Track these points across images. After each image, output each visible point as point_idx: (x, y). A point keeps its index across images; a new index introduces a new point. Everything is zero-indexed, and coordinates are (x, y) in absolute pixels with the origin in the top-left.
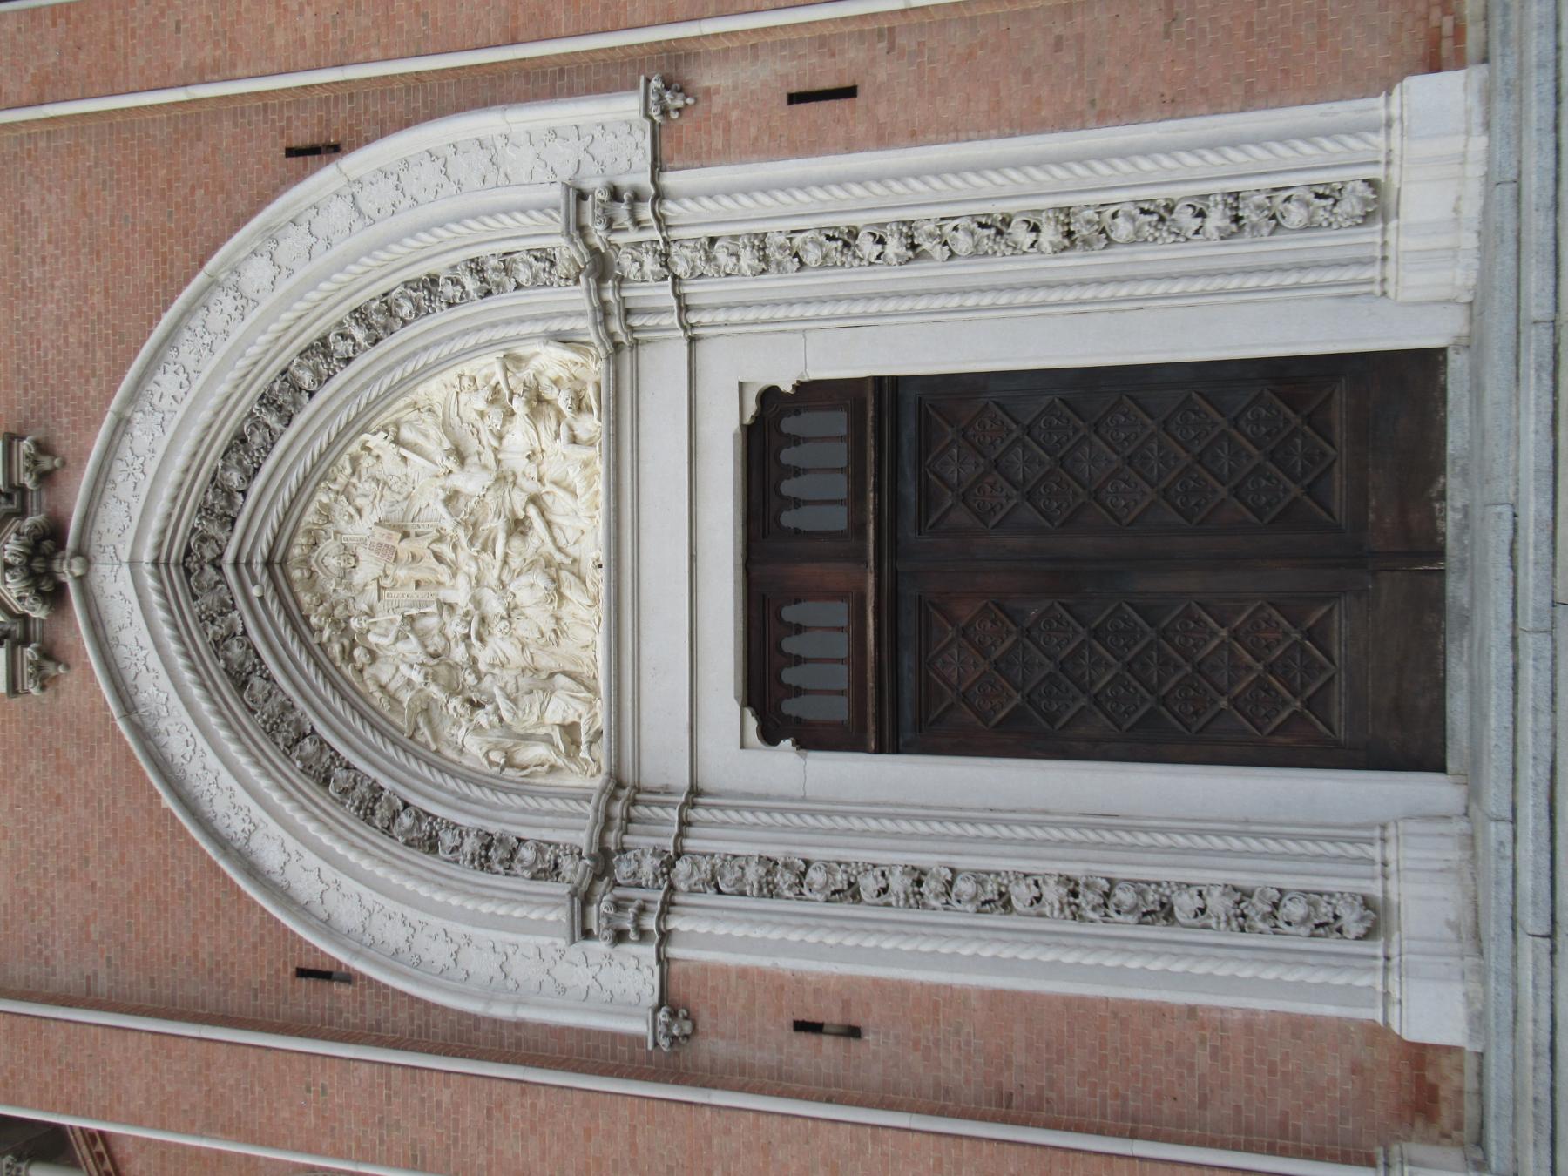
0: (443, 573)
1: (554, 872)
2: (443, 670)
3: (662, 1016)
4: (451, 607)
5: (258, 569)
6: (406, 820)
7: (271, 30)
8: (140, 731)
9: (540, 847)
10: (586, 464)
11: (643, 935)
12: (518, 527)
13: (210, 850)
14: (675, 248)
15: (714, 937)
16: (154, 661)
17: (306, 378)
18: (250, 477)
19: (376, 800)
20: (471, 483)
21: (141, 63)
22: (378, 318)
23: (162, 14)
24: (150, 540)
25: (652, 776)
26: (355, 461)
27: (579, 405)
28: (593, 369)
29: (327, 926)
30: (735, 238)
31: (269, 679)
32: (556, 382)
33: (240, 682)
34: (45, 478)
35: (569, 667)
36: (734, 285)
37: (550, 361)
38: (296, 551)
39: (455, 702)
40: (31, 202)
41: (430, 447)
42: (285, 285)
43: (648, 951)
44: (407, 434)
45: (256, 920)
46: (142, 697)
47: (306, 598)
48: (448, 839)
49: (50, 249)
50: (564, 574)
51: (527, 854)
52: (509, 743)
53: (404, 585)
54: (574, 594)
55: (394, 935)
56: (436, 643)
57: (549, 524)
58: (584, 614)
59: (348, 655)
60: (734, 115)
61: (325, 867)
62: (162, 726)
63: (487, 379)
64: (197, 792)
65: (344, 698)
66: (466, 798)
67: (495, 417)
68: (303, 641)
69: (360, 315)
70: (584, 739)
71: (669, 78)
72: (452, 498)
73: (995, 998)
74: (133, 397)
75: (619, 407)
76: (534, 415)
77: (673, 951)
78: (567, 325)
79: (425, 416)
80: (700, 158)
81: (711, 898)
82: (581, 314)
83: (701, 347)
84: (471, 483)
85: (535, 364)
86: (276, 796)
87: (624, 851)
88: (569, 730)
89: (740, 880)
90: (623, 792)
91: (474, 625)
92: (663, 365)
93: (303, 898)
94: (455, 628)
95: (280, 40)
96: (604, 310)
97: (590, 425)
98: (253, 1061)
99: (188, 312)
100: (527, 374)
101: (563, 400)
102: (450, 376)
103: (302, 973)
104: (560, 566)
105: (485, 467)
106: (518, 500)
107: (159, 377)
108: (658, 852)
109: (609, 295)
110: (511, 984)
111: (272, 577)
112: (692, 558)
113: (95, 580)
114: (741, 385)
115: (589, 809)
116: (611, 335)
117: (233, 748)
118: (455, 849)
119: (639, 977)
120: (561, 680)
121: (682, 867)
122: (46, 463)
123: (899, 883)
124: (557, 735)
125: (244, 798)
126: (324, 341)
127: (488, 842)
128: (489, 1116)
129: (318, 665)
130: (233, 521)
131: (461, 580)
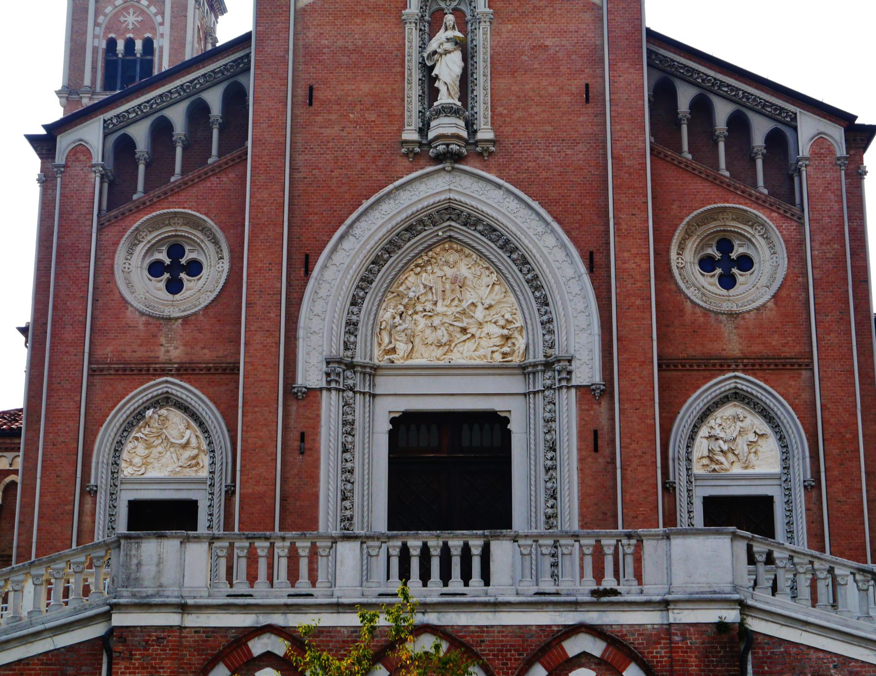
0: (448, 302)
1: (347, 348)
2: (413, 302)
3: (304, 390)
4: (435, 304)
5: (448, 234)
6: (361, 294)
7: (629, 251)
8: (390, 192)
9: (354, 343)
10: (485, 356)
11: (329, 382)
12: (464, 330)
13: (348, 222)
14: (552, 391)
15: (330, 407)
16: (415, 198)
17: (515, 256)
18: (480, 232)
19: (368, 282)
20: (480, 313)
21: (623, 199)
22: (535, 283)
23: (639, 208)
24: (457, 197)
25: (379, 380)
26: (488, 268)
27: (505, 355)
28: (516, 359)
29: (325, 266)
30: (555, 412)
31: (409, 240)
32: (514, 344)
35: (415, 349)
36: (541, 410)
37: (520, 343)
38: (455, 246)
39: (402, 308)
40: (580, 147)
41: (493, 296)
42: (545, 251)
43: (324, 385)
44: (497, 288)
45: (325, 238)
46: (402, 193)
47: (438, 249)
48: (355, 309)
49: (563, 154)
50: (447, 347)
51: (352, 339)
52: (388, 328)
53: (443, 287)
54: (440, 352)
55: (323, 293)
56: (423, 299)
57: (465, 341)
58: (434, 354)
59: (417, 266)
60: (592, 412)
61: (345, 266)
62: (392, 201)
63: (515, 319)
64: (369, 215)
65: (403, 267)
66: (369, 314)
67: (502, 322)
68: (422, 251)
69: (536, 277)
70: (391, 357)
71: (607, 391)
72: (473, 304)
73: (316, 496)
74: (508, 190)
75: (503, 369)
76: (502, 336)
77: (324, 393)
78: (531, 352)
79: (503, 295)
80: (579, 401)
81: (341, 404)
82: (534, 357)
83: (523, 397)
85: (520, 337)
86: (368, 247)
87: (355, 373)
88: (394, 350)
89: (348, 414)
90: (372, 371)
91: (430, 314)
92: (516, 384)
93: (334, 257)
94: (429, 306)
95: (626, 254)
96: (535, 365)
98: (277, 242)
99: (538, 214)
100: (516, 334)
101: (506, 349)
102: (516, 306)
103: (307, 256)
104: (450, 345)
105: (485, 317)
106: (472, 330)
107: (516, 201)
108: (355, 385)
109: (539, 368)
110: (309, 335)
111: (445, 238)
112: (453, 395)
113: (443, 173)
114: (510, 411)
115: (368, 360)
116: (527, 367)
117: (385, 230)
118: (353, 313)
119: (315, 381)
120: (410, 346)
121: (351, 394)
122: (486, 154)
124: (391, 346)
126: (528, 263)
127: (355, 324)
128: (267, 331)
129: (414, 257)
130: (465, 225)
131: (445, 309)
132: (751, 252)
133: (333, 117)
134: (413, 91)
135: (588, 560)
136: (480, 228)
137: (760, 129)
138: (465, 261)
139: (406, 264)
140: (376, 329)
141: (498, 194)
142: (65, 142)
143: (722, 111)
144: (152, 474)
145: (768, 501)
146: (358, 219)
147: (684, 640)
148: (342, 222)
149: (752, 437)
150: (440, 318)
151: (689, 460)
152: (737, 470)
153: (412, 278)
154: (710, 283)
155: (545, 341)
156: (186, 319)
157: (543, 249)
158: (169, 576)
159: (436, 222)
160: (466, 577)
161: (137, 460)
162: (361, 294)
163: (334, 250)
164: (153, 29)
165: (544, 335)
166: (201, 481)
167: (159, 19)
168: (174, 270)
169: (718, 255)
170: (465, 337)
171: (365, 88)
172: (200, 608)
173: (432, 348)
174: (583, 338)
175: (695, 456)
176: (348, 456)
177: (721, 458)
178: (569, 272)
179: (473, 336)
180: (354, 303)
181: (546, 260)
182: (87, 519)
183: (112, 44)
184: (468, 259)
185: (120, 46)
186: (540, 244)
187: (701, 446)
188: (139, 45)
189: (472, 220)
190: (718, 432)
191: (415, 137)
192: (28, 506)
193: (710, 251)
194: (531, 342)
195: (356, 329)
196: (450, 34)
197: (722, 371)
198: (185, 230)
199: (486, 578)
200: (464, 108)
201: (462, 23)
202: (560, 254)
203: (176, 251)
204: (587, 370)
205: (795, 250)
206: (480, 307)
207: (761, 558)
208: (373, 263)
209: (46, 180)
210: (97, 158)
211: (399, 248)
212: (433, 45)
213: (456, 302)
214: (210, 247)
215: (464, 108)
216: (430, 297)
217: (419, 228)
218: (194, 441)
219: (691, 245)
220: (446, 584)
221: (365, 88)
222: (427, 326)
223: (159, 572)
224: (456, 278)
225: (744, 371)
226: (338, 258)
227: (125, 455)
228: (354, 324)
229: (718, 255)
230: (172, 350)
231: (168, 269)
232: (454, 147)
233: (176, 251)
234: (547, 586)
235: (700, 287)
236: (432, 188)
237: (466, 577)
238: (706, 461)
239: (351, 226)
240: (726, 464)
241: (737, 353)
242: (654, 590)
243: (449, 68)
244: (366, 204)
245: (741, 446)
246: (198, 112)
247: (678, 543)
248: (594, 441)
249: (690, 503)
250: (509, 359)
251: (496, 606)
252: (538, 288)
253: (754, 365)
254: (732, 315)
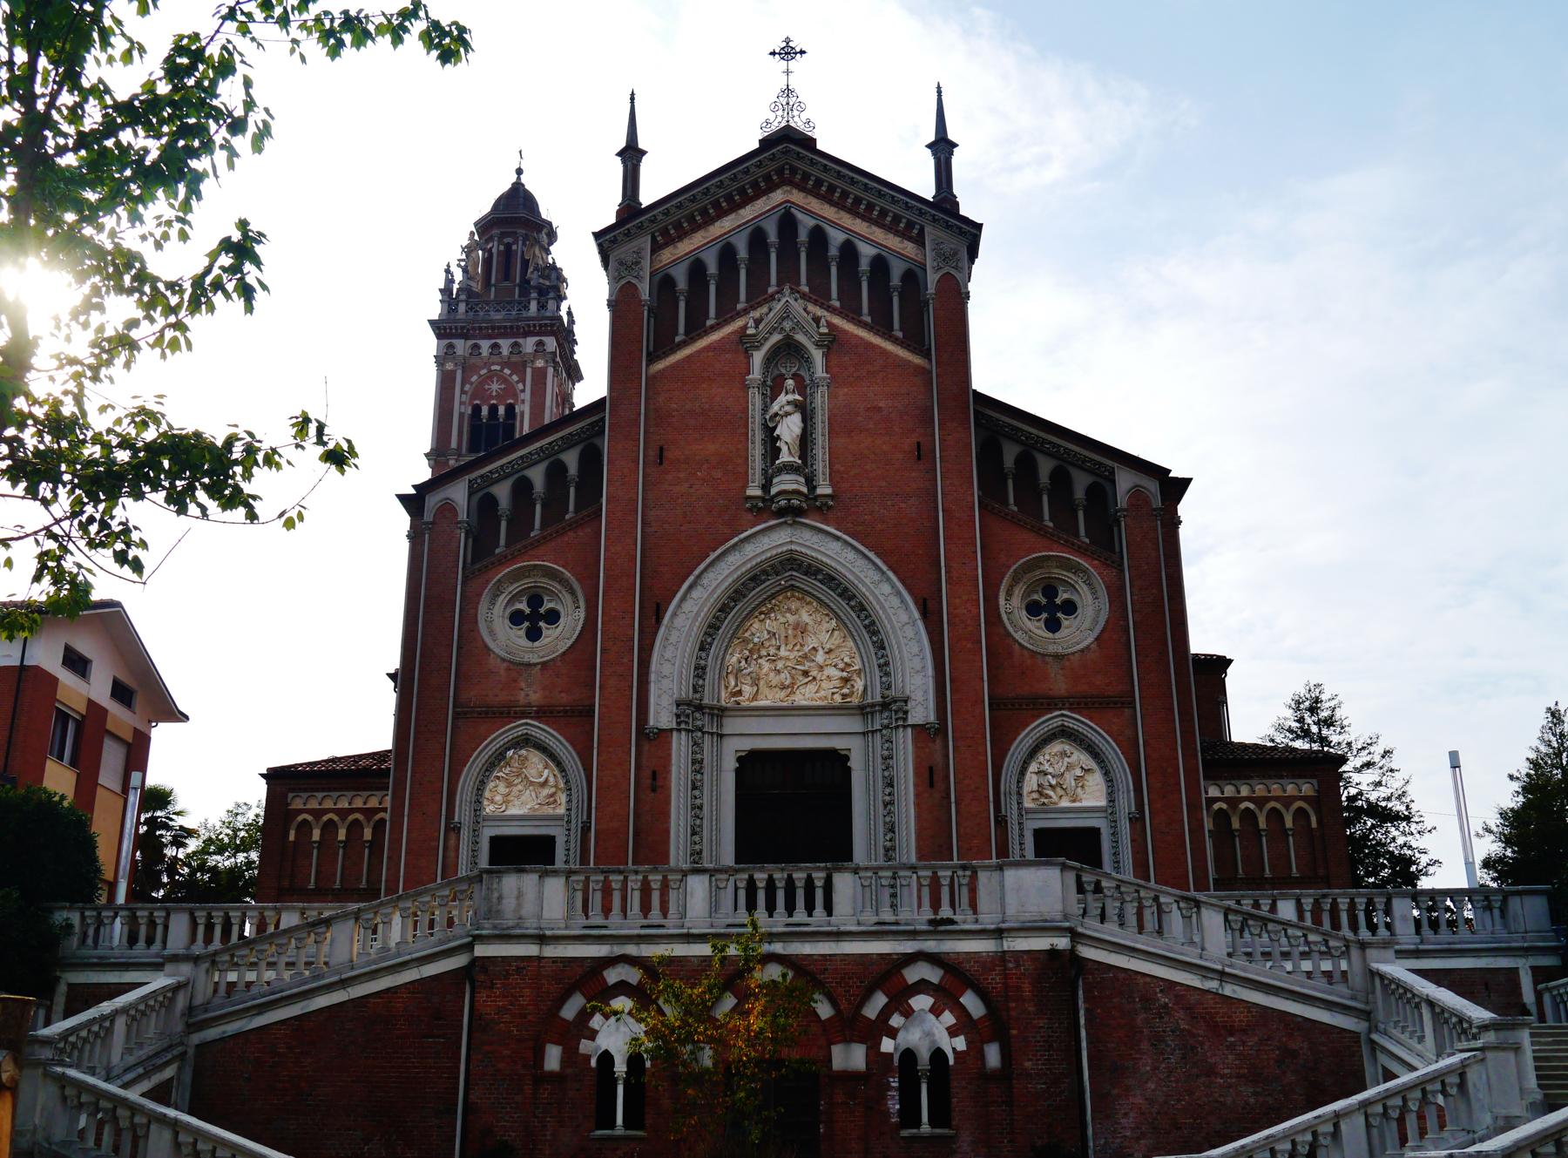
1: (695, 691)
4: (779, 648)
9: (703, 686)
11: (679, 723)
12: (806, 674)
13: (696, 572)
15: (680, 747)
16: (759, 550)
20: (820, 657)
22: (872, 629)
25: (726, 721)
27: (844, 696)
28: (855, 700)
29: (675, 614)
34: (819, 509)
37: (859, 685)
54: (783, 694)
55: (673, 639)
56: (767, 644)
67: (841, 665)
69: (873, 623)
71: (941, 730)
73: (667, 831)
76: (842, 678)
80: (915, 740)
88: (740, 693)
90: (719, 713)
92: (855, 724)
96: (873, 705)
99: (874, 564)
101: (845, 691)
103: (658, 605)
106: (814, 673)
123: (698, 802)
127: (704, 668)
132: (1075, 598)
133: (682, 475)
134: (757, 451)
135: (926, 892)
137: (1081, 483)
141: (836, 546)
142: (432, 501)
143: (1045, 467)
144: (513, 811)
145: (1096, 832)
147: (1018, 966)
148: (690, 573)
149: (1079, 772)
151: (1020, 794)
152: (1065, 803)
153: (756, 625)
154: (1036, 627)
156: (544, 665)
158: (529, 908)
160: (810, 909)
161: (498, 798)
163: (683, 599)
164: (515, 396)
166: (560, 818)
167: (520, 386)
168: (534, 619)
169: (1044, 601)
171: (712, 448)
172: (557, 939)
174: (918, 680)
175: (1026, 790)
176: (697, 793)
177: (1051, 793)
178: (904, 617)
180: (702, 649)
181: (882, 607)
182: (452, 854)
183: (477, 410)
185: (485, 411)
187: (1031, 781)
188: (501, 410)
189: (812, 569)
190: (1046, 767)
191: (758, 492)
192: (396, 842)
193: (1036, 597)
196: (790, 397)
197: (1050, 710)
198: (544, 582)
199: (829, 908)
200: (804, 467)
201: (801, 387)
202: (895, 601)
203: (535, 600)
204: (922, 711)
205: (1116, 595)
206: (821, 652)
207: (1089, 888)
209: (415, 536)
210: (463, 516)
212: (775, 408)
214: (567, 598)
215: (804, 467)
218: (551, 779)
219: (1018, 592)
220: (790, 915)
221: (712, 448)
223: (519, 905)
225: (1070, 709)
226: (687, 606)
227: (487, 794)
229: (1044, 601)
230: (532, 694)
231: (527, 618)
232: (795, 502)
233: (535, 600)
234: (887, 916)
235: (1027, 630)
236: (774, 541)
237: (810, 909)
238: (1035, 795)
239: (699, 577)
240: (1055, 798)
241: (1063, 692)
242: (988, 920)
243: (789, 429)
244: (713, 556)
245: (1069, 781)
246: (557, 472)
247: (1010, 874)
248: (930, 777)
249: (1021, 835)
251: (838, 935)
252: (875, 633)
253: (1079, 703)
254: (1057, 657)
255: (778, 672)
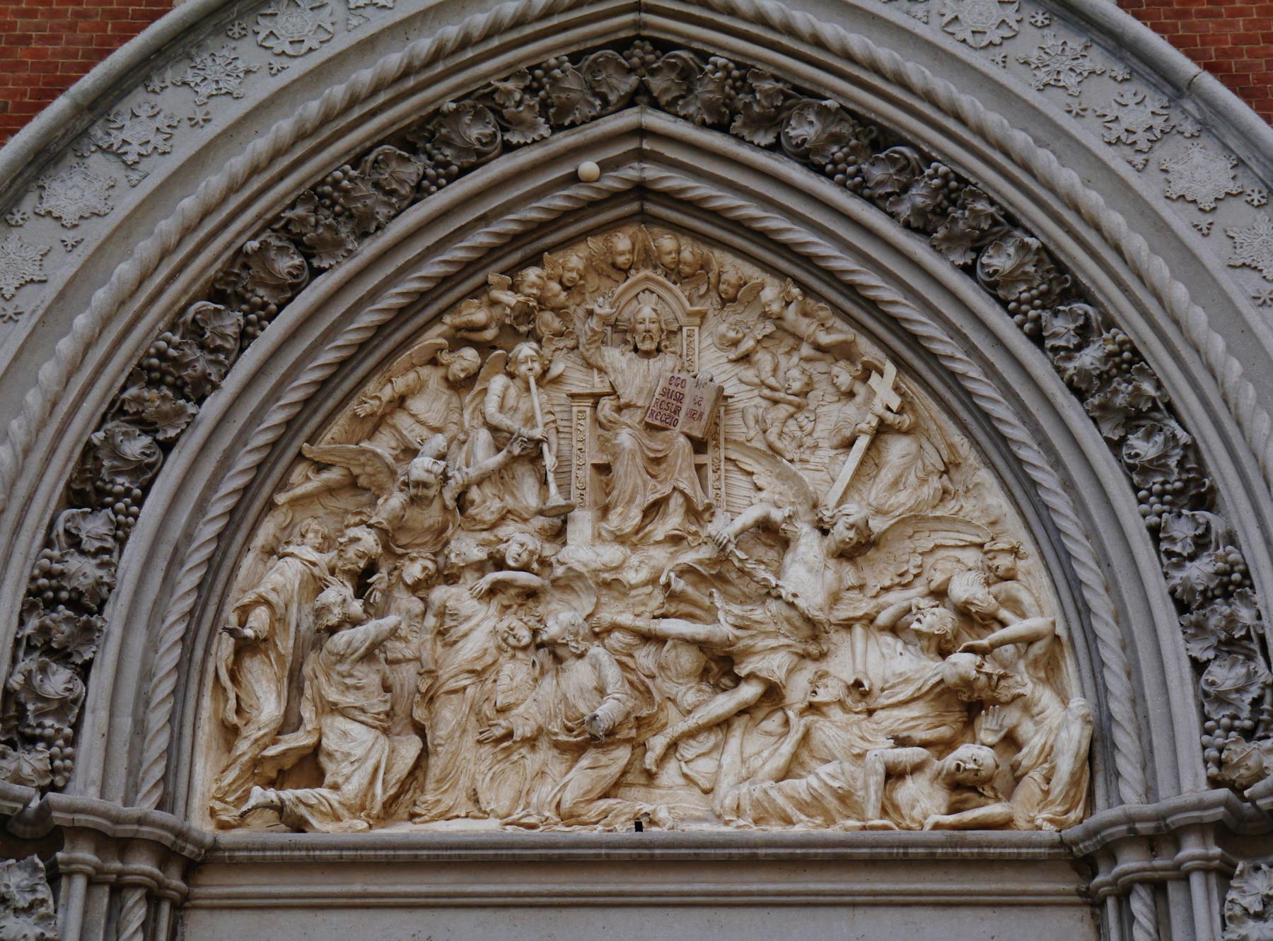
0: (627, 518)
2: (432, 516)
4: (558, 534)
5: (632, 172)
6: (136, 447)
9: (71, 708)
10: (844, 798)
12: (720, 665)
17: (1001, 260)
18: (804, 156)
19: (179, 390)
20: (806, 575)
22: (1124, 396)
26: (843, 352)
27: (963, 787)
28: (1034, 814)
31: (420, 192)
32: (1011, 741)
33: (408, 139)
35: (436, 765)
37: (1056, 724)
38: (667, 242)
39: (369, 541)
41: (876, 492)
42: (1179, 219)
44: (897, 450)
47: (575, 260)
48: (95, 526)
50: (622, 755)
51: (58, 681)
52: (286, 644)
54: (580, 777)
56: (487, 504)
57: (723, 724)
58: (545, 792)
59: (462, 338)
61: (49, 292)
64: (202, 58)
66: (176, 560)
67: (936, 619)
68: (490, 254)
70: (288, 794)
72: (771, 533)
78: (1127, 765)
79: (936, 483)
82: (1150, 792)
84: (806, 575)
85: (1046, 698)
86: (189, 204)
87: (54, 877)
88: (309, 767)
91: (523, 578)
94: (518, 541)
96: (1163, 835)
97: (924, 804)
100: (1024, 682)
101: (975, 753)
102: (1014, 532)
104: (640, 747)
106: (771, 662)
109: (1192, 849)
111: (615, 197)
115: (146, 806)
116: (1110, 851)
117: (283, 126)
118: (75, 542)
120: (410, 748)
124: (299, 740)
125: (187, 144)
126: (1078, 292)
127: (88, 605)
129: (445, 282)
130: (722, 127)
131: (612, 553)
136: (804, 130)
138: (723, 325)
139: (401, 314)
140: (217, 640)
146: (140, 72)
150: (586, 604)
153: (430, 405)
155: (1209, 698)
157: (1168, 212)
159: (566, 108)
162: (136, 447)
165: (1199, 667)
170: (724, 704)
173: (533, 761)
179: (773, 694)
180: (85, 492)
181: (1188, 261)
184: (733, 316)
186: (1148, 187)
194: (1120, 708)
195: (88, 633)
206: (809, 546)
208: (215, 293)
211: (365, 227)
213: (673, 521)
216: (529, 496)
217: (475, 132)
222: (507, 646)
224: (671, 398)
228: (76, 603)
250: (994, 810)
255: (553, 653)
